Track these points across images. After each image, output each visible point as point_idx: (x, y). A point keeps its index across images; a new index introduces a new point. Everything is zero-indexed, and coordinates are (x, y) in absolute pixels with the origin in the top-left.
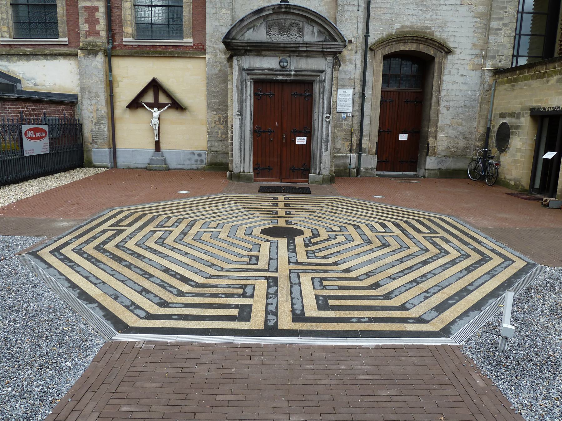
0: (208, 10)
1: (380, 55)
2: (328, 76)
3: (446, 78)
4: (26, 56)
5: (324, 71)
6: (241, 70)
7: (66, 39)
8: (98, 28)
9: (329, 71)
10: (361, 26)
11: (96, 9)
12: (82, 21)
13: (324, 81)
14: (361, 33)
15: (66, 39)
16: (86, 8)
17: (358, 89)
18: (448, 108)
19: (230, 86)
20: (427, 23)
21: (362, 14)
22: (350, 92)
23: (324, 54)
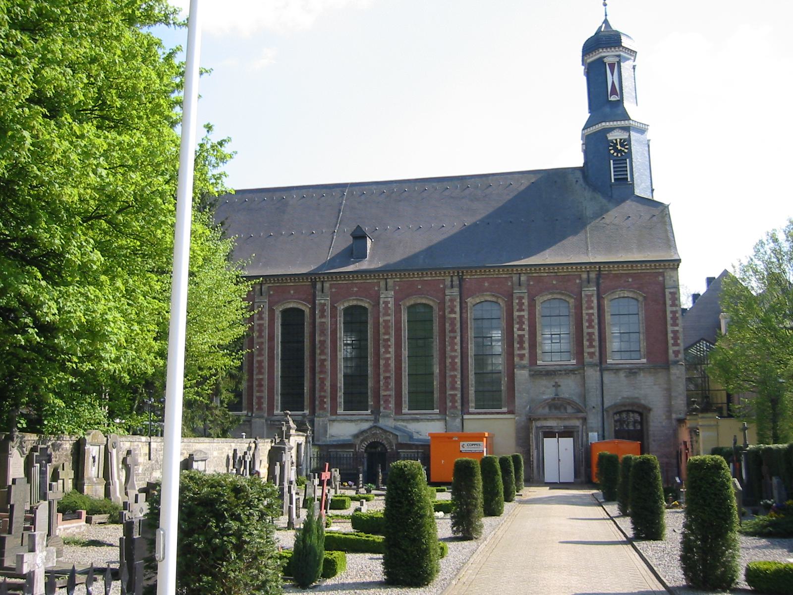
0: (516, 394)
1: (611, 413)
2: (580, 429)
3: (651, 424)
4: (417, 420)
5: (578, 427)
6: (537, 428)
7: (438, 411)
8: (456, 404)
9: (581, 426)
10: (600, 399)
11: (456, 395)
12: (448, 401)
13: (578, 431)
14: (599, 403)
15: (438, 411)
16: (451, 395)
17: (600, 432)
18: (654, 441)
19: (531, 435)
20: (636, 395)
21: (599, 393)
22: (596, 434)
23: (578, 418)
